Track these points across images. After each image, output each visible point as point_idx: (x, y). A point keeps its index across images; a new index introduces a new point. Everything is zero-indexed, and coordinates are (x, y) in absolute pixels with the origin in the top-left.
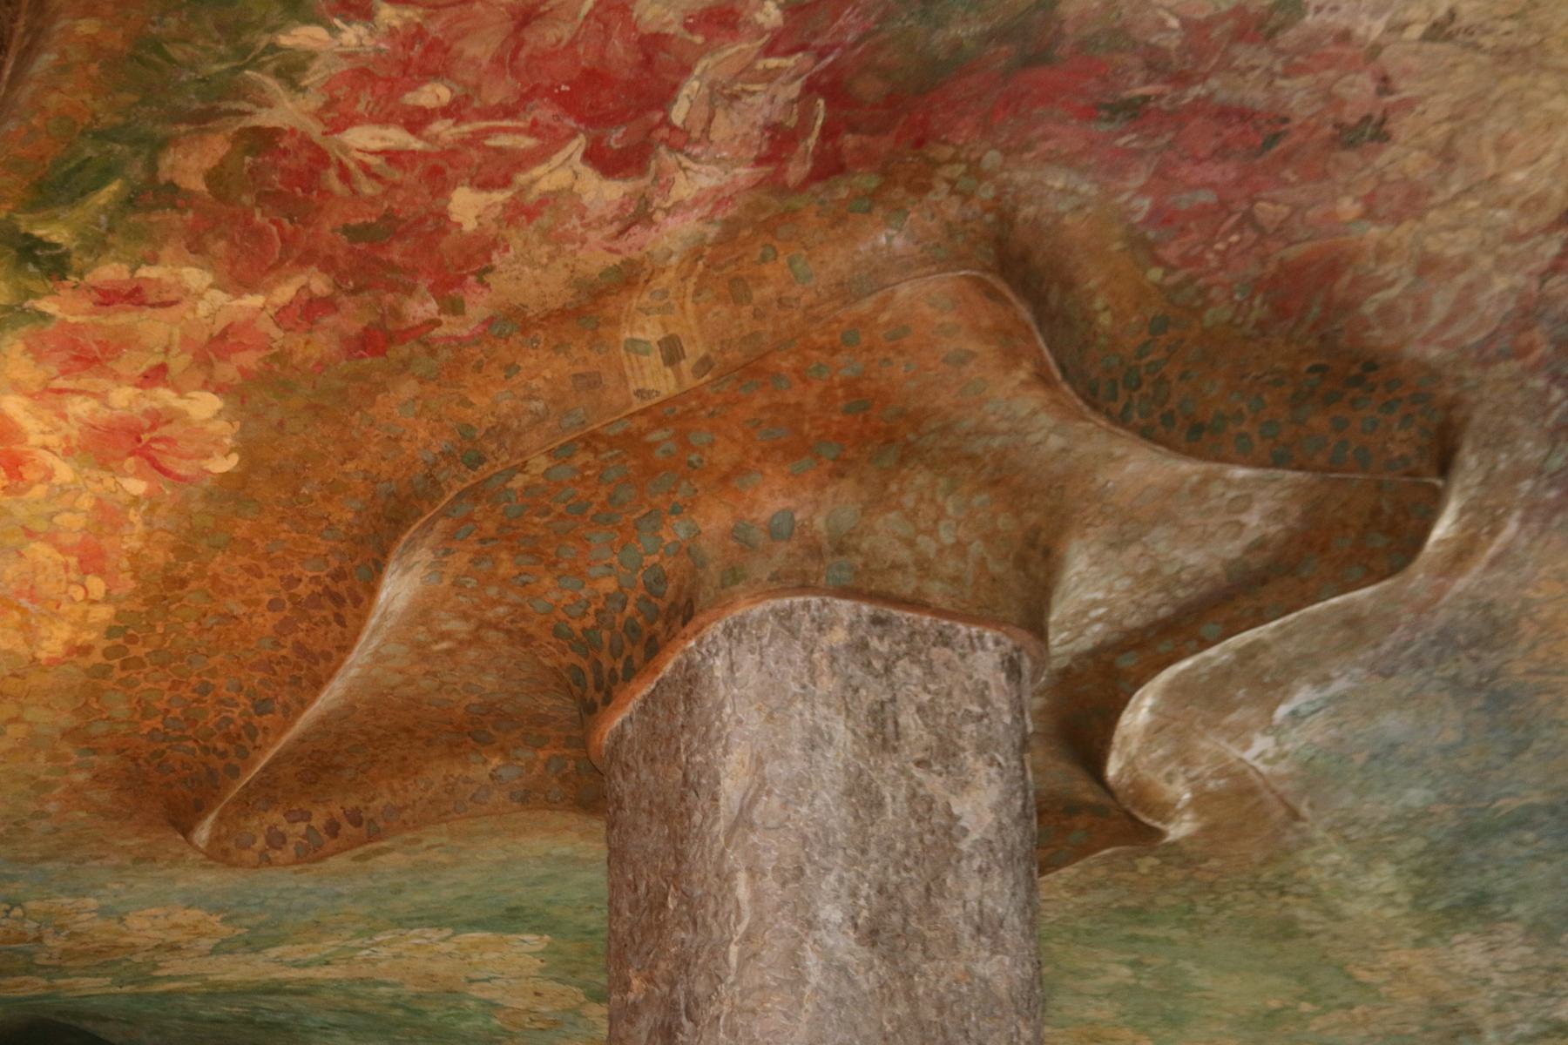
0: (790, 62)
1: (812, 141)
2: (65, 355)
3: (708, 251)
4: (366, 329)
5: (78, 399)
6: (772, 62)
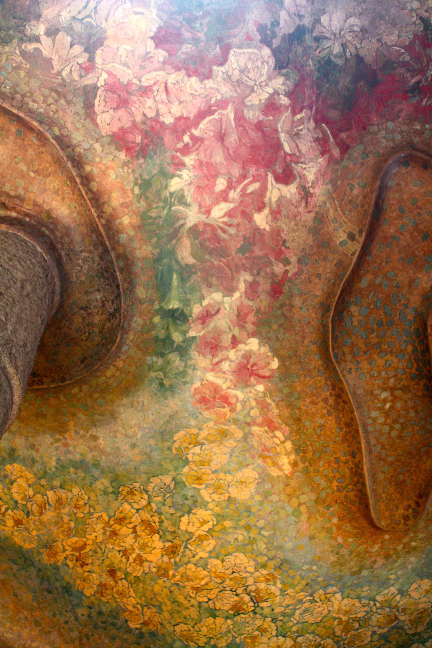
0: (303, 114)
1: (332, 140)
2: (208, 349)
3: (334, 196)
4: (271, 286)
5: (223, 363)
6: (299, 116)
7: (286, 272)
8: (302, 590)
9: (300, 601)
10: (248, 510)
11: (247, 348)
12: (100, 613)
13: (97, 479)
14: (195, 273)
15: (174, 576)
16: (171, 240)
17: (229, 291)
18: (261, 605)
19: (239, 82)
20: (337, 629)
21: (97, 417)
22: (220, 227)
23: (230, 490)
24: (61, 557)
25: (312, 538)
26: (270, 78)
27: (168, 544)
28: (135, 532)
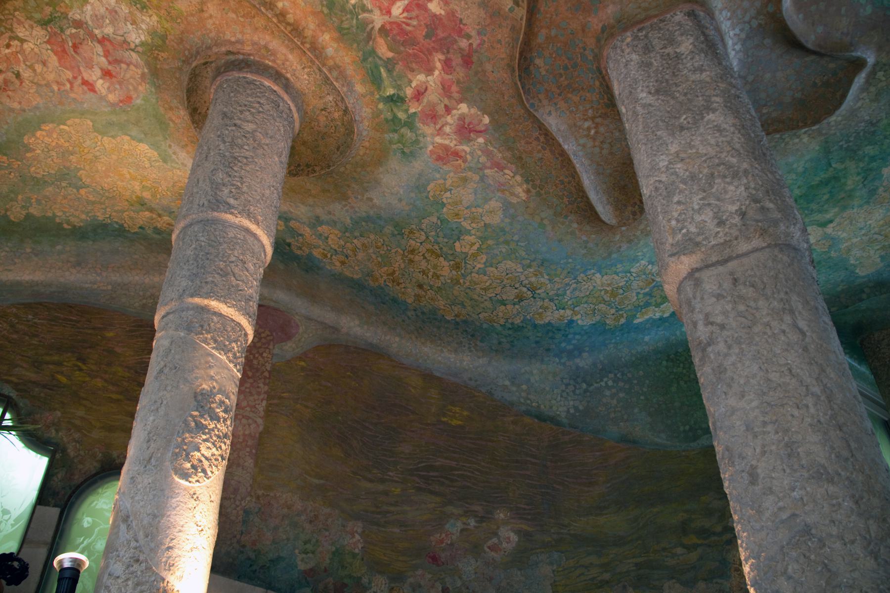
2: (429, 120)
7: (471, 45)
8: (566, 277)
9: (567, 285)
10: (502, 230)
11: (460, 112)
12: (423, 313)
13: (384, 227)
14: (397, 63)
15: (465, 283)
16: (368, 42)
17: (430, 71)
18: (537, 292)
20: (605, 297)
21: (365, 185)
22: (404, 22)
23: (484, 218)
24: (382, 281)
25: (560, 241)
27: (452, 263)
28: (425, 258)
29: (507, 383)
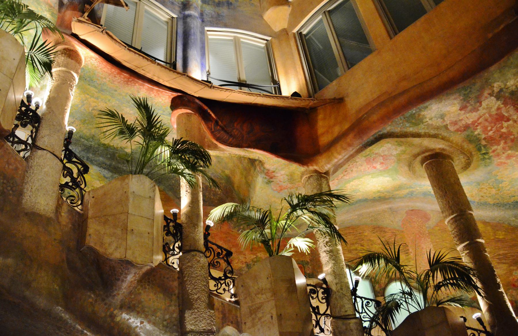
19: (487, 108)
26: (496, 103)
29: (514, 219)
